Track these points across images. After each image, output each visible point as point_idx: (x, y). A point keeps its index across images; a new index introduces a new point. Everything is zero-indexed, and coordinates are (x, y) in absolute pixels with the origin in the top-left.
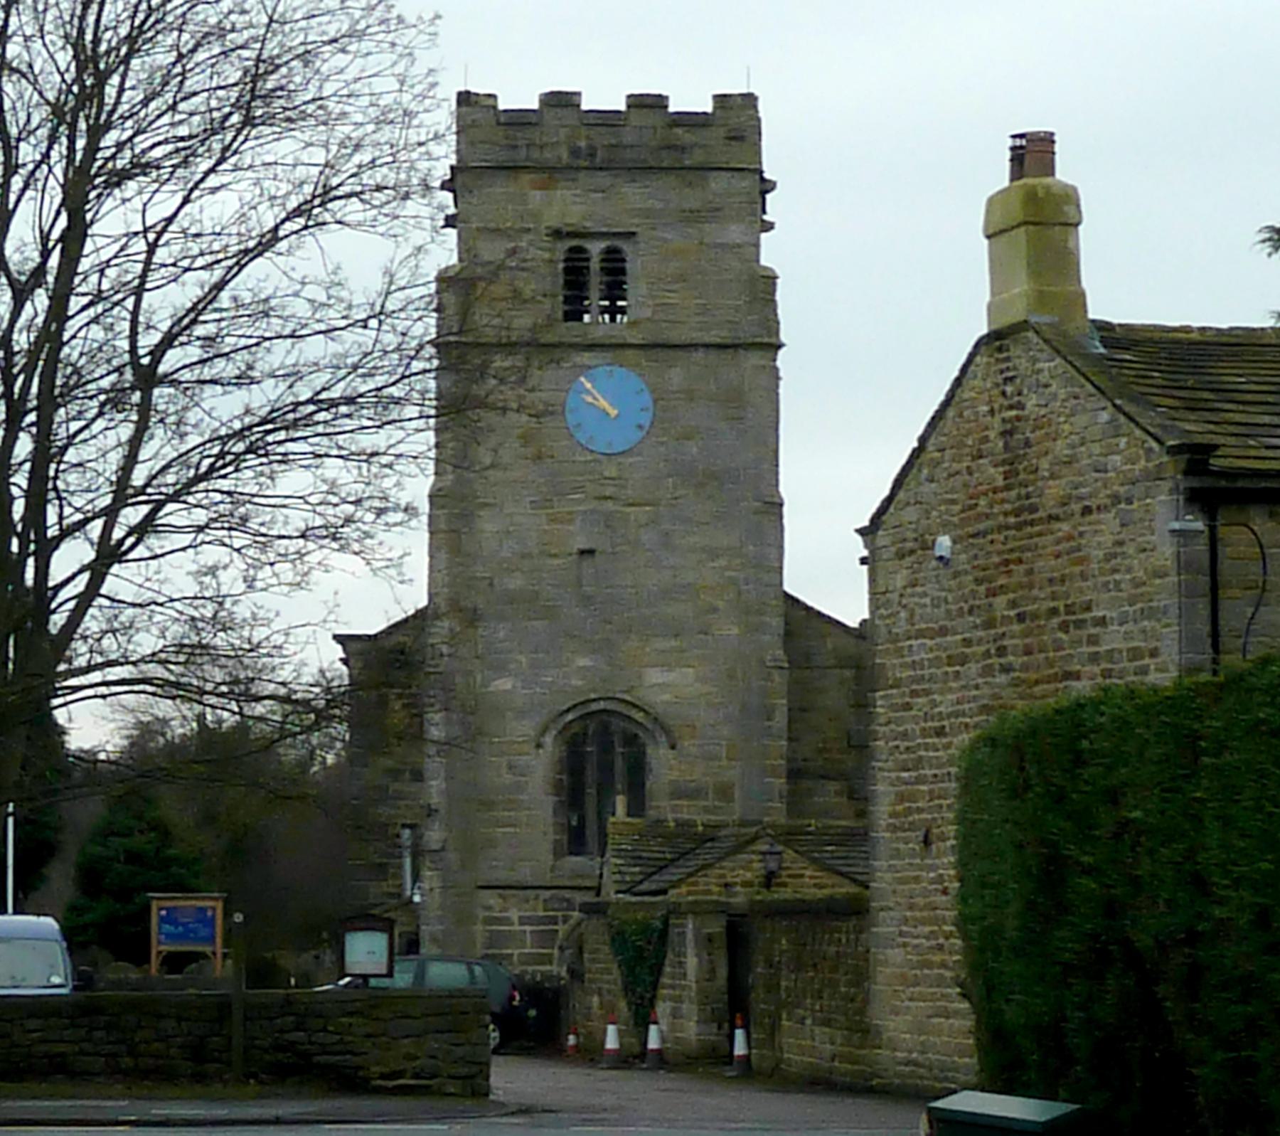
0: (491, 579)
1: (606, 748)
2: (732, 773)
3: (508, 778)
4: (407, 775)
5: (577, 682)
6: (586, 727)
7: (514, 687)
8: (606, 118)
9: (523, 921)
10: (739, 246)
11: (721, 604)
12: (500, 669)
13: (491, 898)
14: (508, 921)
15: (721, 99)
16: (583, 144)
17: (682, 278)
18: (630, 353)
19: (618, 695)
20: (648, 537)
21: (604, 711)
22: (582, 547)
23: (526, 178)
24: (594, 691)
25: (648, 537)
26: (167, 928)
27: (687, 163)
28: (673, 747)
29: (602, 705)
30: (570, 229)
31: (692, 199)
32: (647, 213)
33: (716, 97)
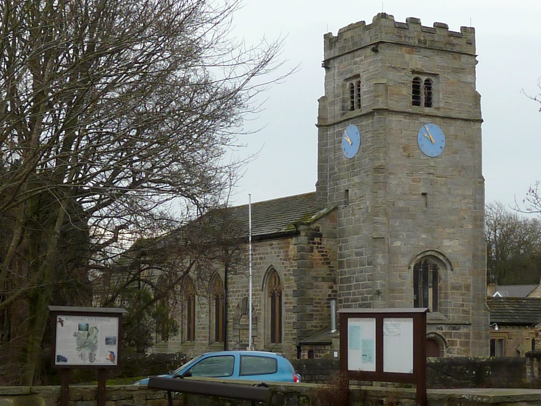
0: (394, 202)
1: (426, 269)
2: (470, 281)
3: (399, 280)
4: (320, 280)
5: (422, 244)
7: (401, 244)
8: (427, 30)
10: (470, 83)
11: (466, 216)
12: (396, 237)
15: (464, 29)
16: (422, 38)
17: (453, 93)
18: (437, 119)
19: (436, 250)
20: (444, 189)
21: (431, 255)
22: (424, 192)
23: (404, 49)
24: (427, 247)
25: (444, 189)
27: (455, 50)
28: (452, 270)
29: (430, 253)
30: (417, 70)
31: (456, 64)
32: (442, 67)
33: (462, 27)
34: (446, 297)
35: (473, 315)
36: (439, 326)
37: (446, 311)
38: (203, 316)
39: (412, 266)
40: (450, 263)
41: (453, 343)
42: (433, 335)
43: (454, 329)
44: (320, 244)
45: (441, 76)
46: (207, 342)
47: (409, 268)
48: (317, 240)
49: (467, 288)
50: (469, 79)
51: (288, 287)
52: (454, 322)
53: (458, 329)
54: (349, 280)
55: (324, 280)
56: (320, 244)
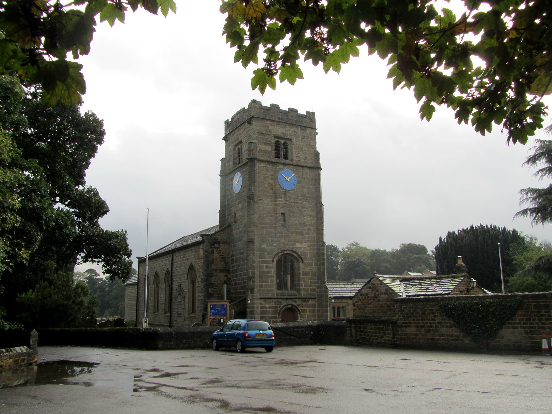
3: (266, 270)
6: (281, 258)
9: (269, 307)
11: (312, 228)
13: (262, 302)
14: (266, 308)
15: (307, 112)
26: (213, 311)
28: (303, 262)
29: (287, 252)
34: (299, 281)
35: (317, 292)
36: (295, 300)
37: (299, 290)
38: (162, 296)
39: (275, 260)
40: (301, 258)
41: (304, 311)
42: (290, 306)
43: (305, 301)
44: (219, 248)
45: (294, 140)
46: (163, 312)
47: (273, 261)
48: (216, 245)
49: (314, 274)
50: (312, 143)
51: (199, 277)
52: (305, 297)
53: (308, 301)
54: (236, 271)
55: (221, 271)
56: (219, 248)
